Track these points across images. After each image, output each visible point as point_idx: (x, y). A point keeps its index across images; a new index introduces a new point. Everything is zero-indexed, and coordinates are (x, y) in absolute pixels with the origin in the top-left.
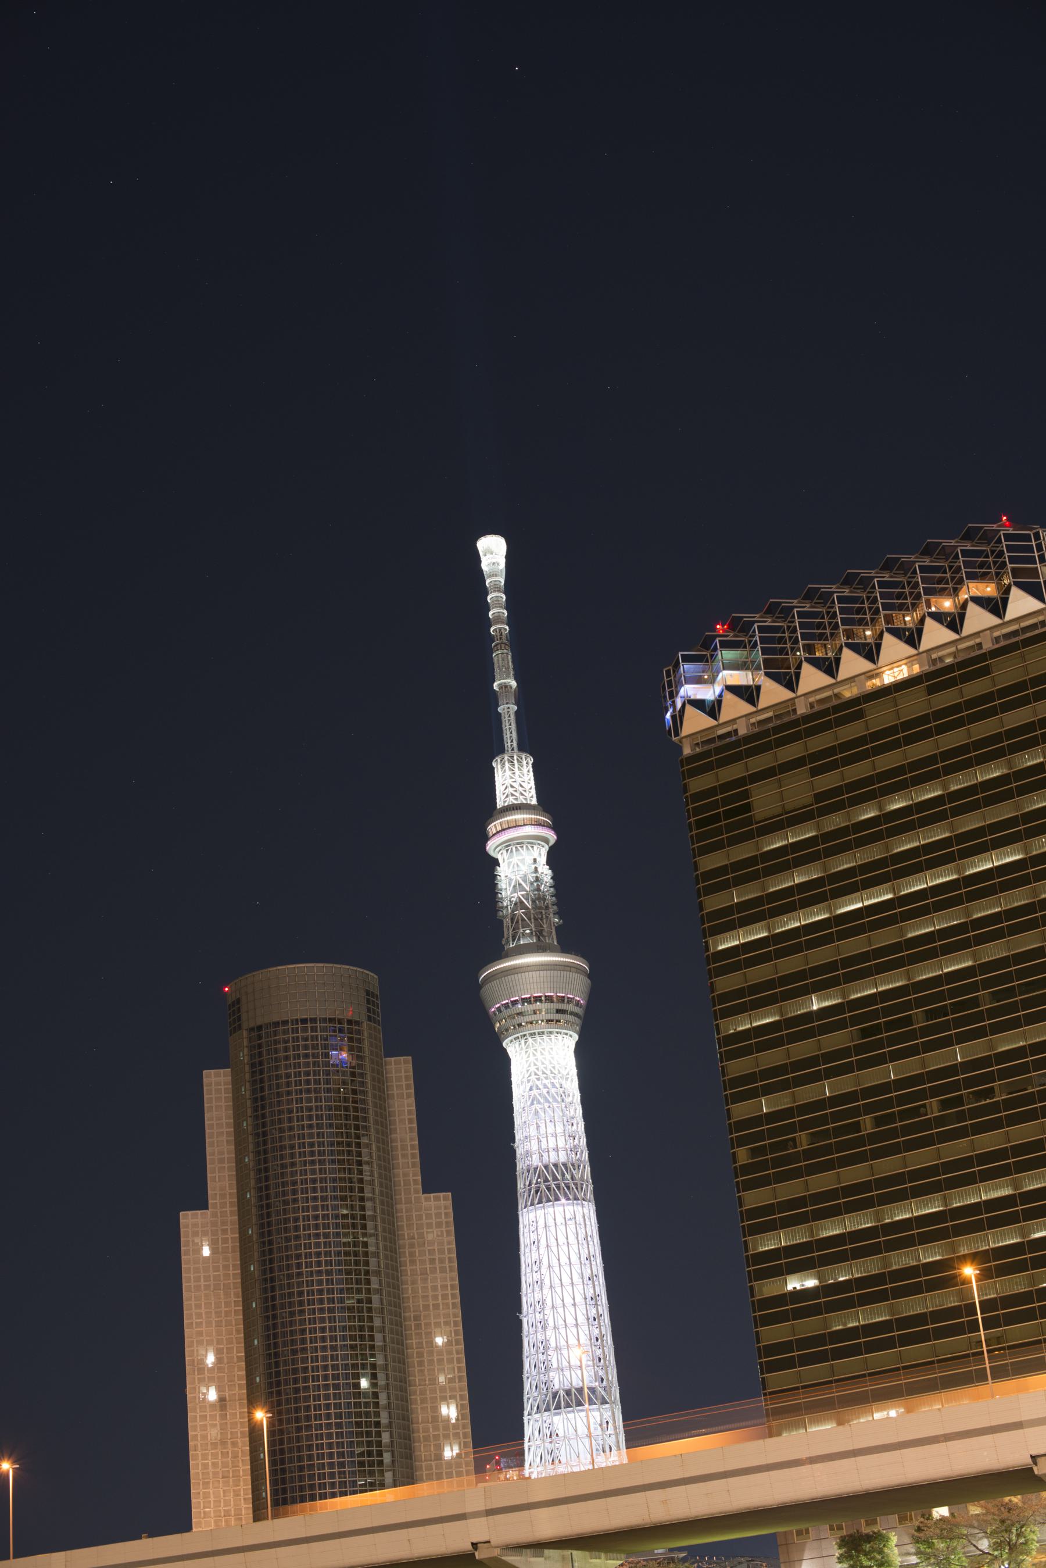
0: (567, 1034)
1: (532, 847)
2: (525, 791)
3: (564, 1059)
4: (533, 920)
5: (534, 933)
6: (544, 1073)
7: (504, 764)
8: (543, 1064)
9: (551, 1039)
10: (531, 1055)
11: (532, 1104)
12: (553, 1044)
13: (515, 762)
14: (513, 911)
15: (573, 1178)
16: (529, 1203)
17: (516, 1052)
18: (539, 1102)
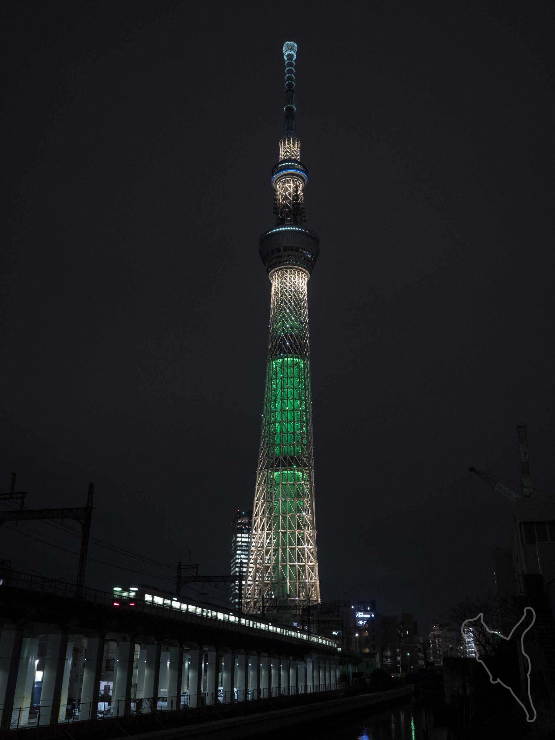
0: (304, 272)
1: (296, 181)
2: (295, 155)
3: (302, 284)
4: (292, 214)
5: (292, 220)
6: (290, 288)
7: (286, 141)
8: (290, 283)
9: (295, 273)
10: (284, 279)
11: (281, 303)
12: (296, 275)
13: (292, 141)
14: (281, 210)
15: (300, 343)
16: (273, 355)
17: (276, 278)
18: (285, 302)
